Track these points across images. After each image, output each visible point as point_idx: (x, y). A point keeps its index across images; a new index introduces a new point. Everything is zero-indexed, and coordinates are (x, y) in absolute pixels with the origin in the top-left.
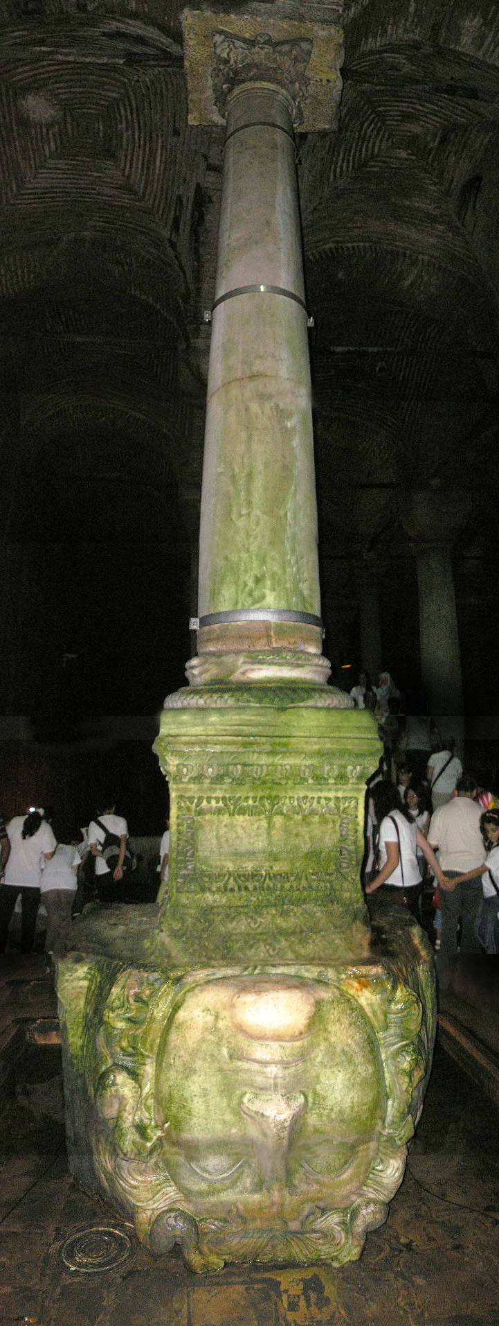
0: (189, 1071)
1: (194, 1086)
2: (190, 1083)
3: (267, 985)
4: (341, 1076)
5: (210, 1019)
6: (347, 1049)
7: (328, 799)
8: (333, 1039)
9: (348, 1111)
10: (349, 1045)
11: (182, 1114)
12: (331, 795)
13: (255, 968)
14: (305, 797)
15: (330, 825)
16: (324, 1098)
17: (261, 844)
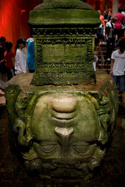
0: (39, 121)
1: (41, 125)
2: (40, 124)
3: (62, 96)
5: (45, 105)
6: (86, 115)
7: (83, 40)
8: (82, 112)
9: (87, 134)
10: (87, 114)
11: (37, 133)
12: (84, 38)
13: (60, 91)
14: (76, 39)
15: (84, 48)
16: (79, 129)
17: (62, 54)
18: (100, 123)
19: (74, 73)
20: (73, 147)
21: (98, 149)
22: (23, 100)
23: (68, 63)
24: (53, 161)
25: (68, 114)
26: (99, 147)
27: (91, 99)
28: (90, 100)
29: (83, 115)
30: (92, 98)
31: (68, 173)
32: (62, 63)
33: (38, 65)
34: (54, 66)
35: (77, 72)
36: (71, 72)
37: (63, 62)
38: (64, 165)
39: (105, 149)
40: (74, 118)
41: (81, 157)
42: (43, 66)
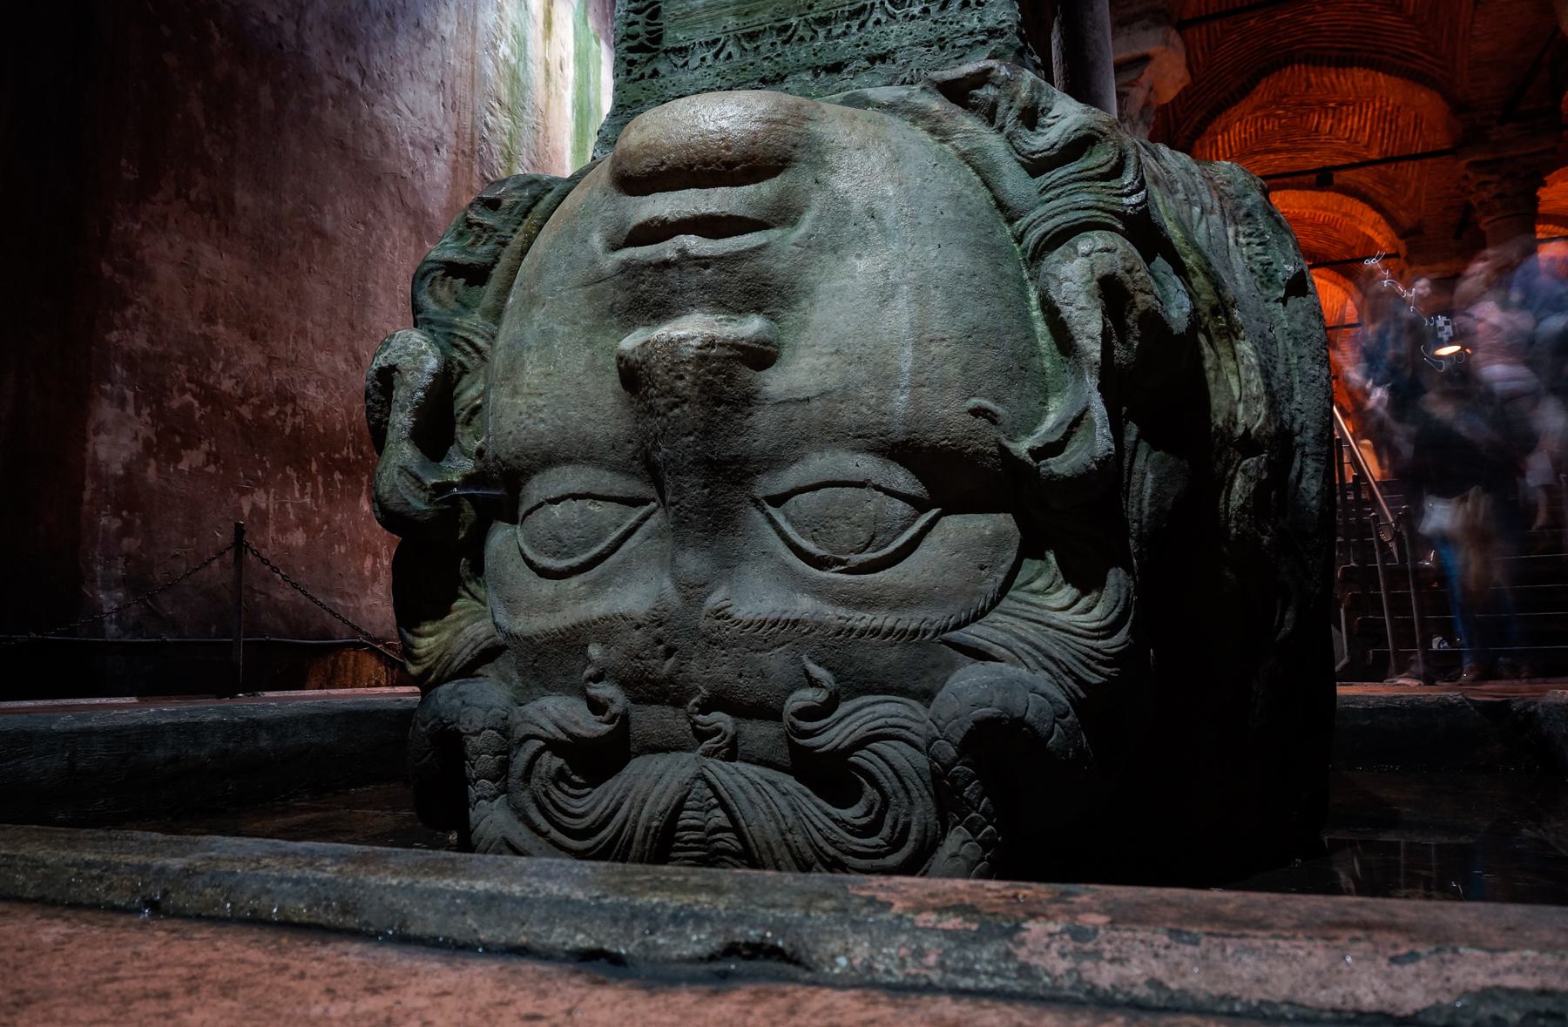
4: (861, 265)
6: (879, 205)
8: (841, 184)
18: (1041, 327)
19: (866, 64)
20: (771, 509)
21: (1038, 584)
22: (472, 215)
23: (823, 22)
24: (594, 651)
25: (719, 190)
26: (1051, 557)
27: (947, 125)
28: (939, 132)
29: (847, 203)
30: (952, 117)
31: (723, 805)
32: (788, 27)
33: (632, 63)
34: (730, 56)
35: (883, 58)
36: (837, 68)
37: (794, 21)
38: (679, 703)
39: (1115, 577)
40: (774, 234)
41: (832, 614)
42: (663, 67)
